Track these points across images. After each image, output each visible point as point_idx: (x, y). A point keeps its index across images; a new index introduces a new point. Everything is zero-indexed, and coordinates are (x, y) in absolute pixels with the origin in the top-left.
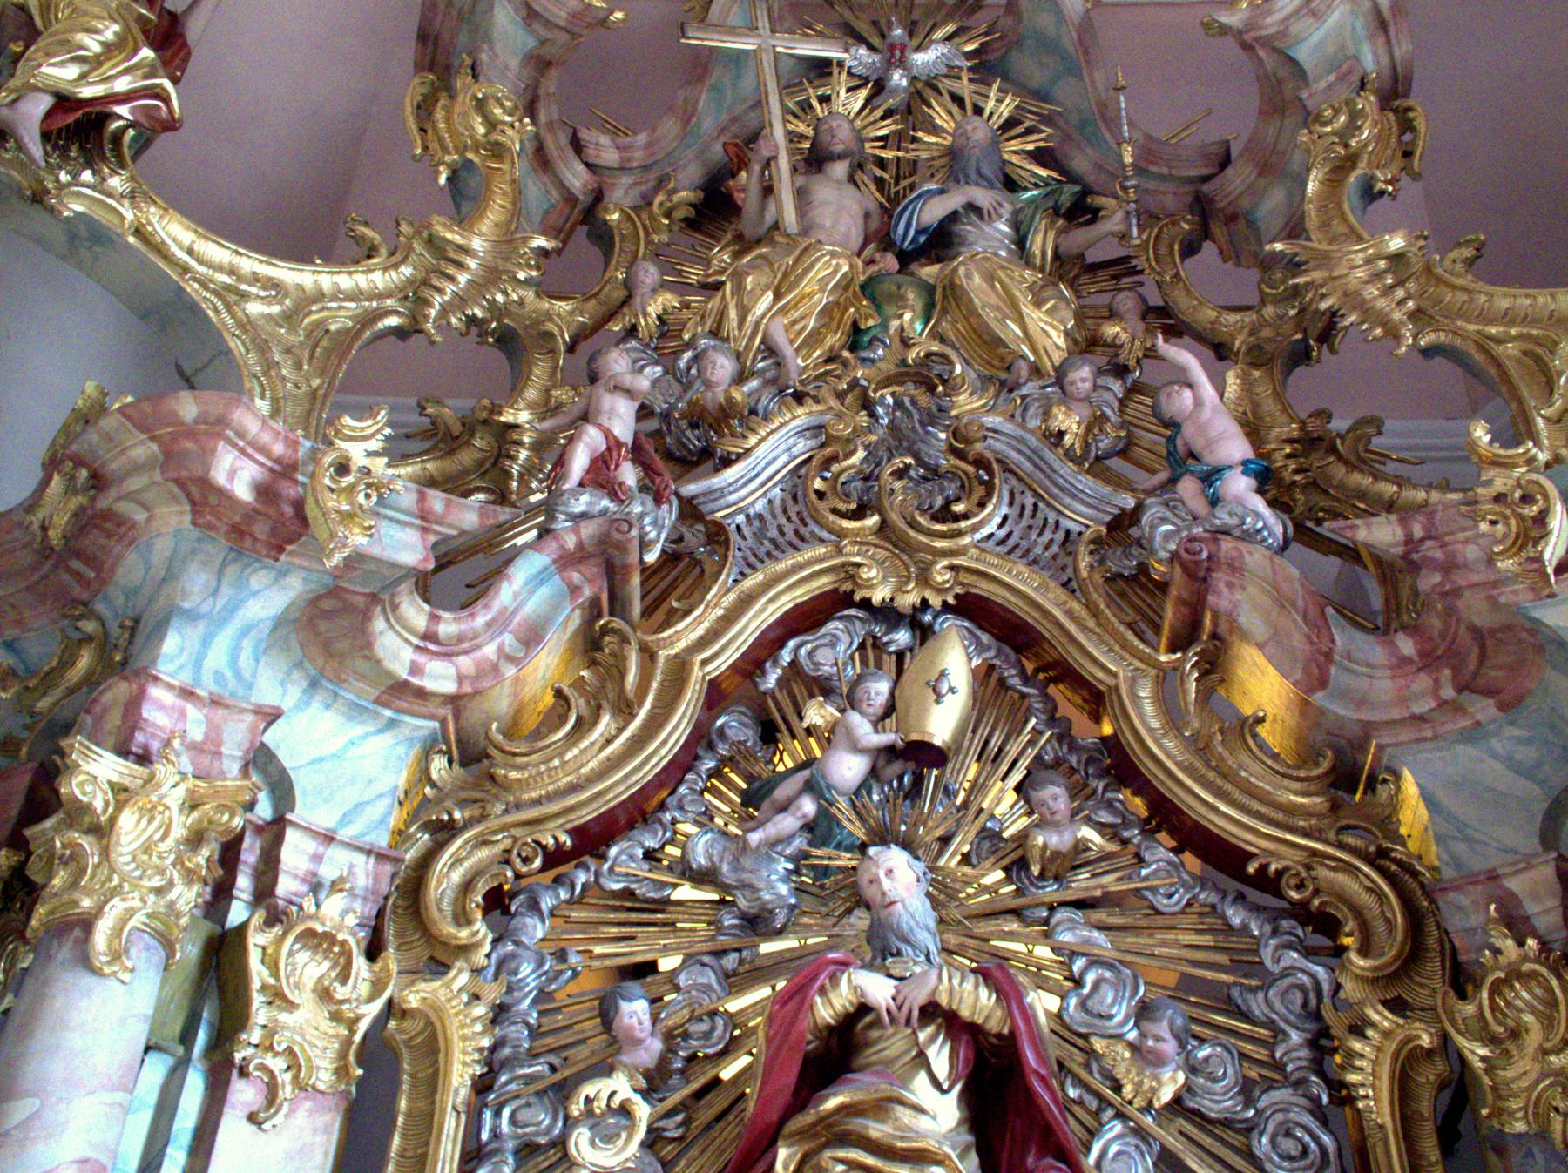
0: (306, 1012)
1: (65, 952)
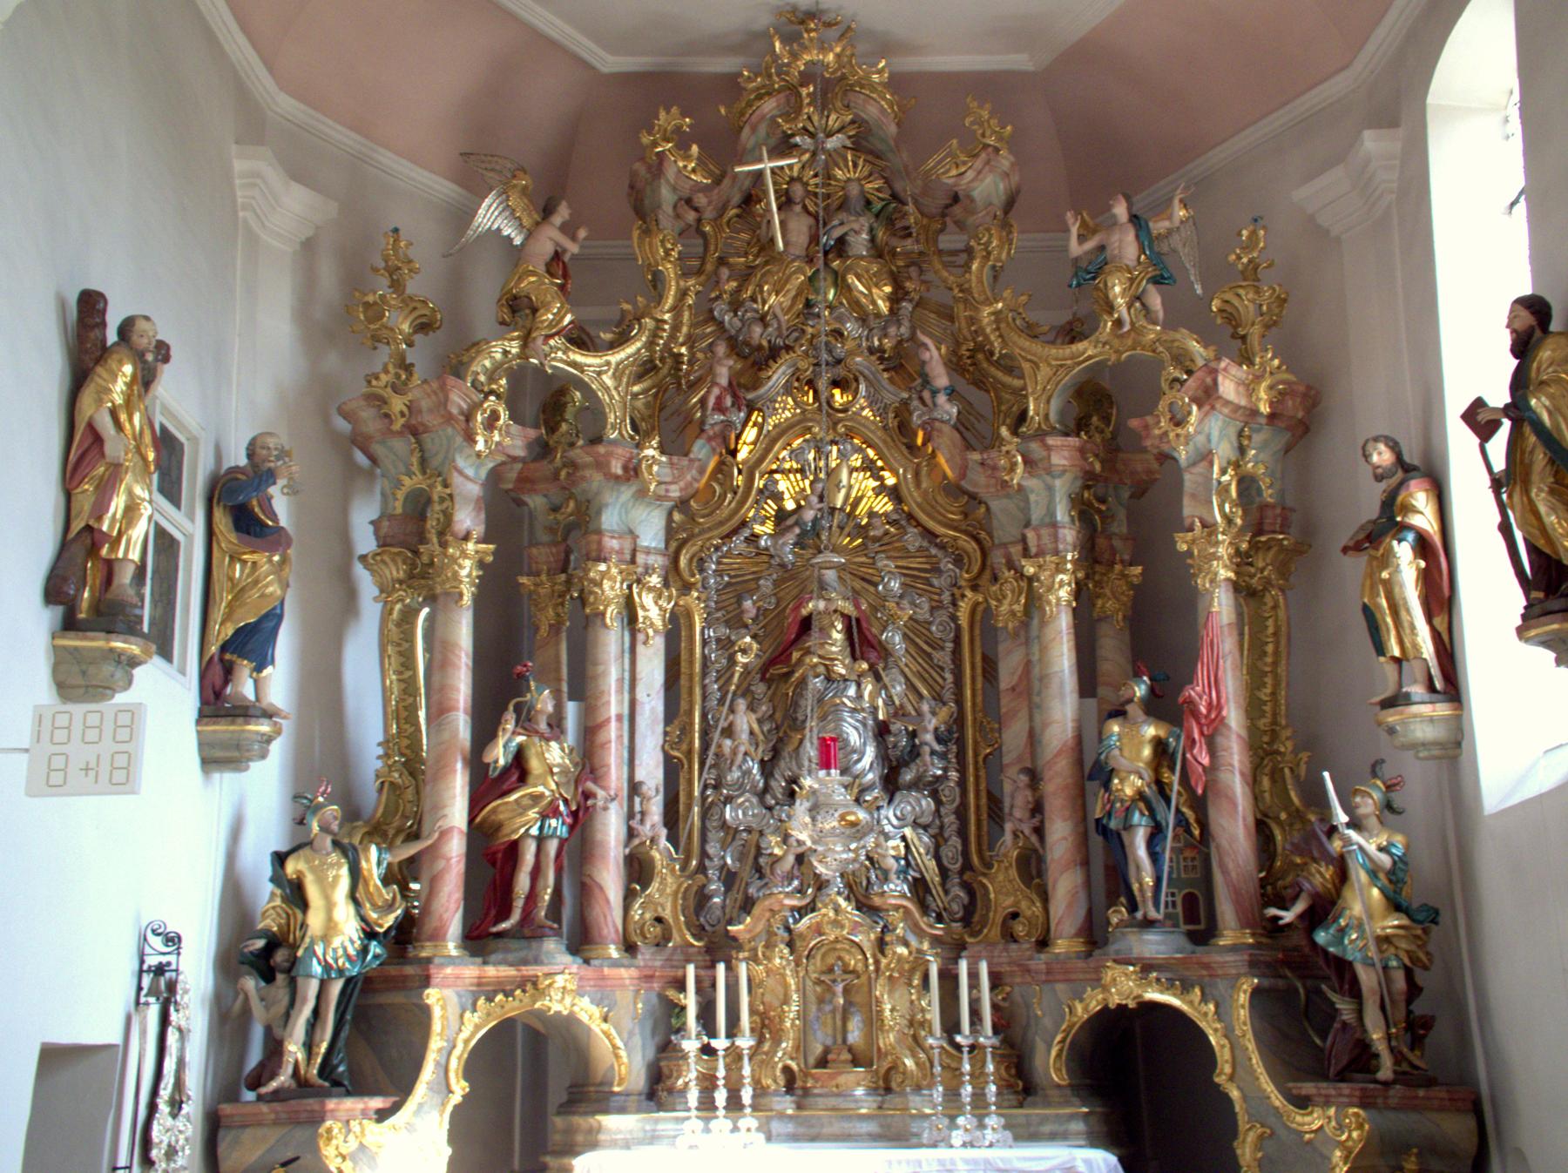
0: (652, 610)
1: (599, 622)
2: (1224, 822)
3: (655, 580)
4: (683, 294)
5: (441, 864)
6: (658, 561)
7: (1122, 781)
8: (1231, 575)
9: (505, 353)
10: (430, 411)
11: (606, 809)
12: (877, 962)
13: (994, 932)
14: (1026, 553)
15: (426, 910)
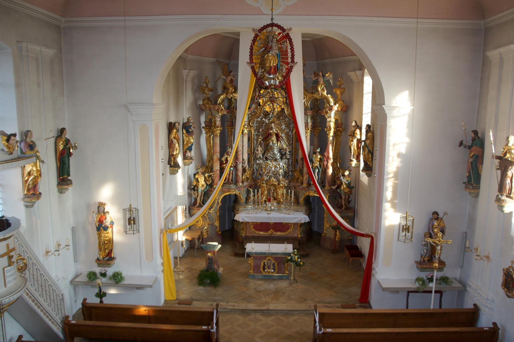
0: (246, 131)
13: (295, 181)
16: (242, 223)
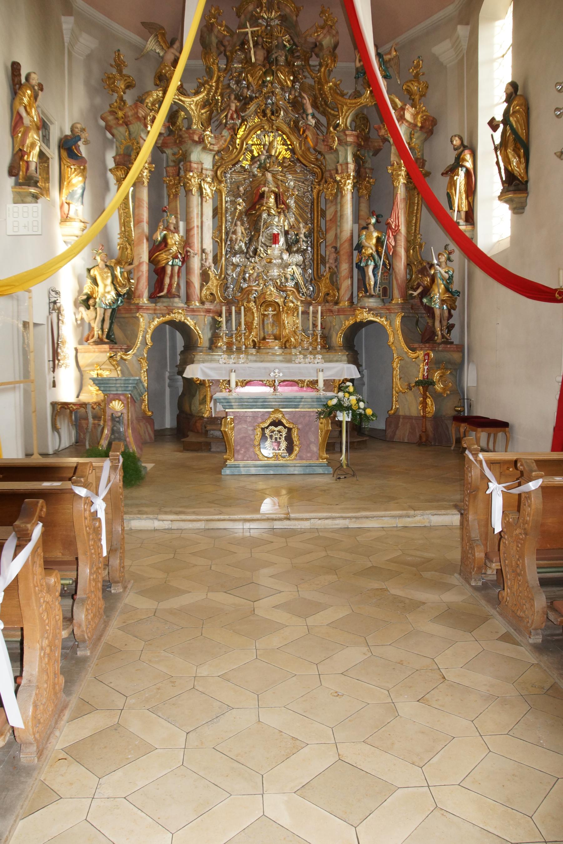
0: (208, 190)
1: (190, 193)
2: (397, 264)
3: (209, 180)
4: (219, 77)
5: (140, 273)
6: (210, 173)
7: (365, 250)
8: (405, 182)
9: (157, 95)
10: (132, 116)
11: (194, 257)
12: (283, 308)
14: (337, 173)
15: (136, 288)
16: (203, 383)
